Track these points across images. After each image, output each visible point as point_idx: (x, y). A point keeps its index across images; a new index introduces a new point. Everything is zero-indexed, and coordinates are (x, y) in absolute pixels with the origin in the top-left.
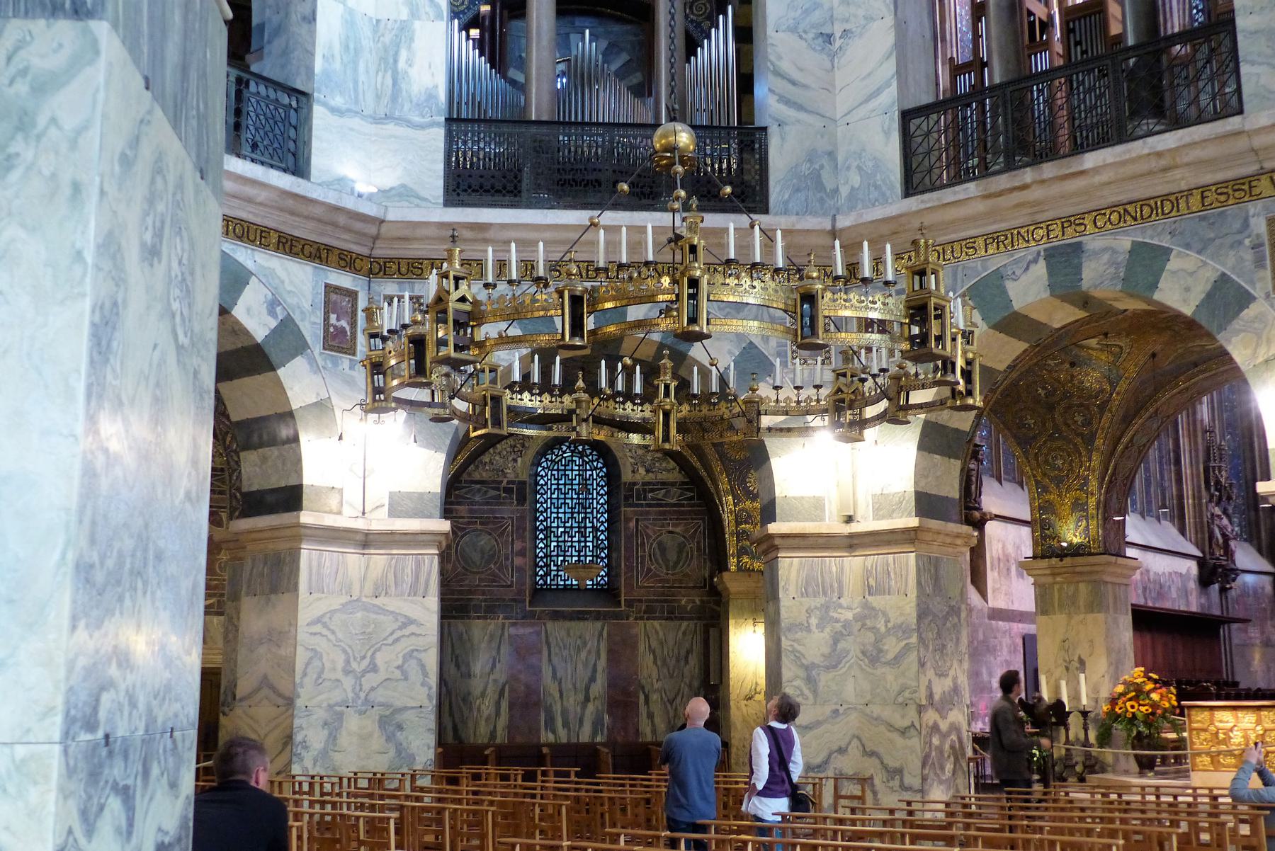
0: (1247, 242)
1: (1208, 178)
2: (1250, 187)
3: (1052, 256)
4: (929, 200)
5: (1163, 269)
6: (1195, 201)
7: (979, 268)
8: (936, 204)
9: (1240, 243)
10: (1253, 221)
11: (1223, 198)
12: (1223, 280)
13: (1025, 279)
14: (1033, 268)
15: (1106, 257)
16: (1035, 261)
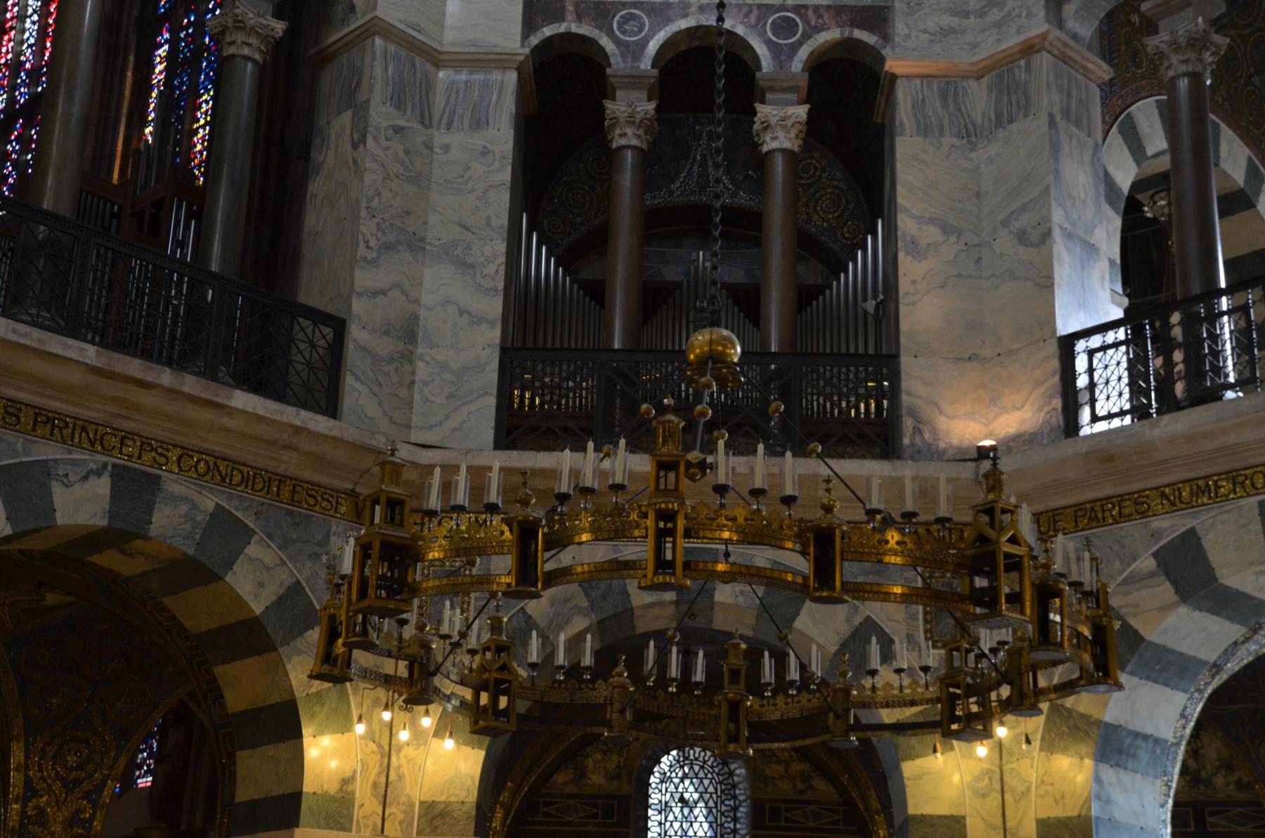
0: (324, 558)
1: (306, 475)
2: (337, 503)
3: (119, 475)
4: (25, 335)
5: (240, 552)
6: (286, 491)
7: (19, 446)
8: (35, 345)
9: (318, 556)
10: (333, 539)
11: (311, 501)
12: (296, 589)
13: (79, 490)
14: (92, 479)
15: (184, 509)
16: (99, 473)
